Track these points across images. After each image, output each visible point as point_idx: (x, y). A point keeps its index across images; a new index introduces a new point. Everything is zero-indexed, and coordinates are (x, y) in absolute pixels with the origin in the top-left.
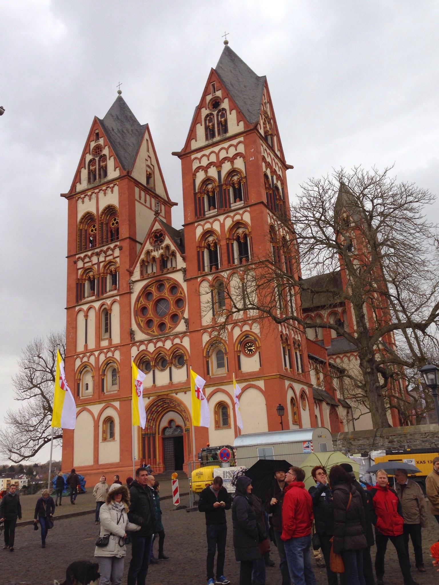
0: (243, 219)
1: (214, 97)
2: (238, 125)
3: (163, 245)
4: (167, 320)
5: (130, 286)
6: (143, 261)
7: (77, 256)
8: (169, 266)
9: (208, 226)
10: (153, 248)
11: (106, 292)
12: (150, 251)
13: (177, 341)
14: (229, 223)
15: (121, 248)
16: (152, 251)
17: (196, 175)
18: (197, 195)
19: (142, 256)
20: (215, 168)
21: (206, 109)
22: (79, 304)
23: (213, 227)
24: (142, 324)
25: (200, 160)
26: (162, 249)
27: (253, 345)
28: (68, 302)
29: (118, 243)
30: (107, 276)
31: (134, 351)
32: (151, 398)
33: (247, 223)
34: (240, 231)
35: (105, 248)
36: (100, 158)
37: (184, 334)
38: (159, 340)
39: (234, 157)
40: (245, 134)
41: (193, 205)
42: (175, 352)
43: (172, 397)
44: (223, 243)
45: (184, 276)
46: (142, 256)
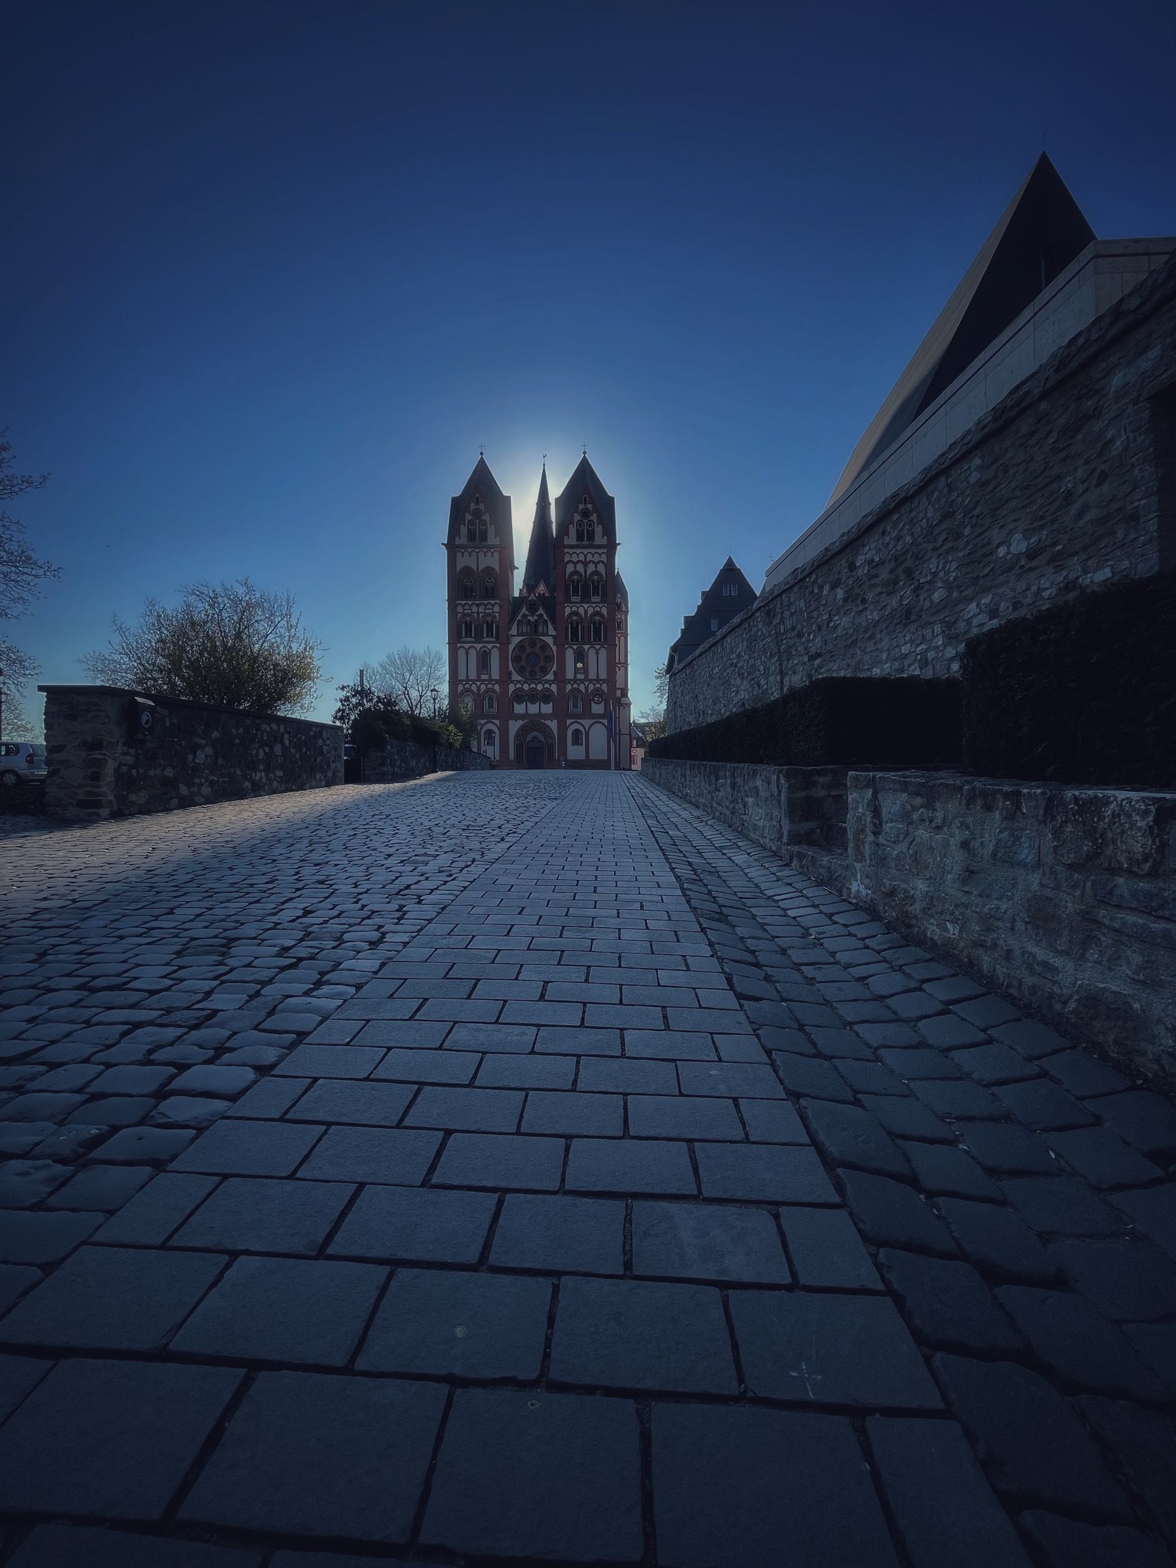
3: (537, 613)
4: (537, 669)
6: (519, 622)
7: (458, 602)
8: (541, 630)
9: (574, 609)
11: (483, 638)
13: (547, 685)
14: (590, 611)
15: (501, 606)
24: (517, 669)
25: (571, 555)
29: (498, 601)
31: (512, 688)
32: (525, 721)
34: (597, 618)
35: (486, 602)
36: (479, 522)
37: (553, 682)
44: (586, 625)
46: (519, 618)
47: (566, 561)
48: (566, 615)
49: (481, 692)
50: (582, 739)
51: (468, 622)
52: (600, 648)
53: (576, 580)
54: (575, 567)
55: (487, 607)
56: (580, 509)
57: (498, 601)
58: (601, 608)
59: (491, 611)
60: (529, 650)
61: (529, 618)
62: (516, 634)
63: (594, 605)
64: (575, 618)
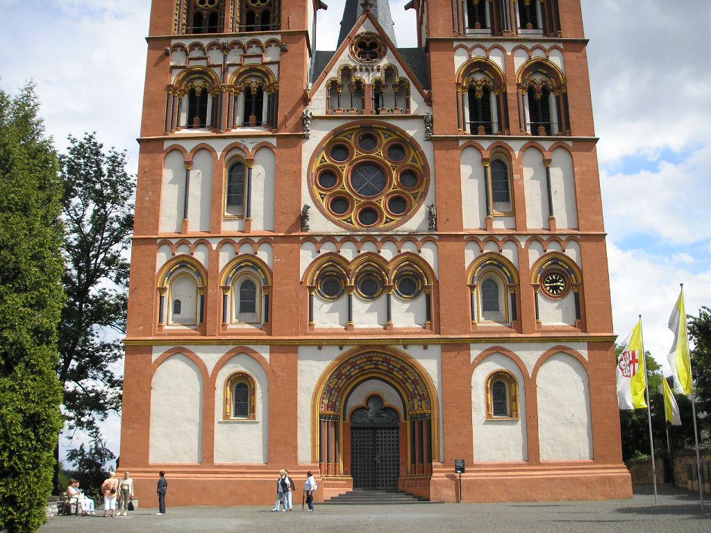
0: (551, 59)
3: (384, 63)
4: (383, 202)
5: (304, 125)
7: (173, 42)
9: (478, 54)
11: (234, 128)
12: (351, 68)
13: (408, 248)
14: (520, 61)
16: (355, 69)
19: (334, 74)
22: (171, 136)
26: (378, 70)
27: (560, 279)
28: (145, 127)
30: (239, 94)
32: (346, 349)
34: (538, 78)
35: (245, 40)
37: (428, 239)
38: (369, 239)
42: (402, 267)
43: (396, 351)
45: (427, 130)
46: (334, 74)
48: (456, 72)
49: (221, 268)
50: (514, 399)
51: (198, 90)
52: (552, 149)
55: (250, 52)
57: (279, 37)
59: (256, 61)
60: (357, 154)
61: (358, 75)
62: (324, 115)
63: (529, 46)
64: (479, 77)
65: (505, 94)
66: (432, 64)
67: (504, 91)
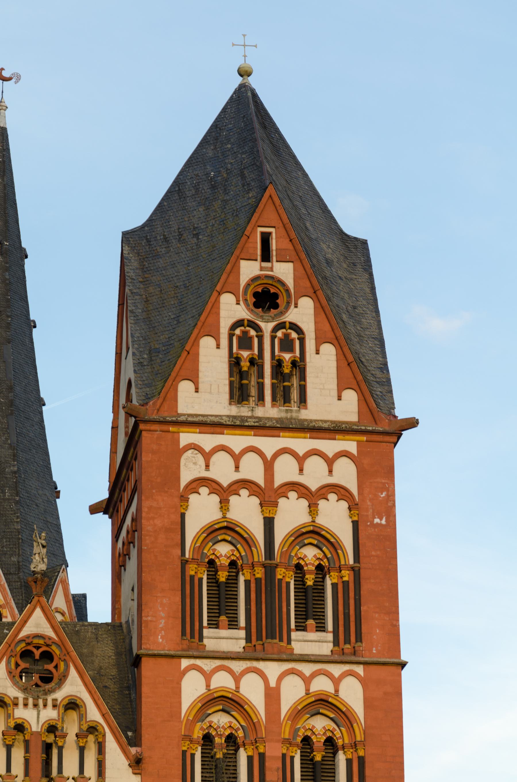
0: (343, 694)
1: (267, 277)
2: (339, 398)
3: (60, 695)
10: (20, 695)
12: (6, 700)
16: (16, 705)
17: (187, 500)
18: (187, 566)
20: (255, 501)
21: (238, 303)
23: (242, 690)
25: (207, 456)
26: (54, 706)
33: (349, 709)
39: (324, 491)
40: (364, 438)
41: (178, 599)
47: (183, 483)
53: (226, 562)
54: (224, 504)
56: (244, 279)
58: (336, 682)
63: (307, 669)
65: (262, 756)
66: (143, 699)
67: (261, 750)
